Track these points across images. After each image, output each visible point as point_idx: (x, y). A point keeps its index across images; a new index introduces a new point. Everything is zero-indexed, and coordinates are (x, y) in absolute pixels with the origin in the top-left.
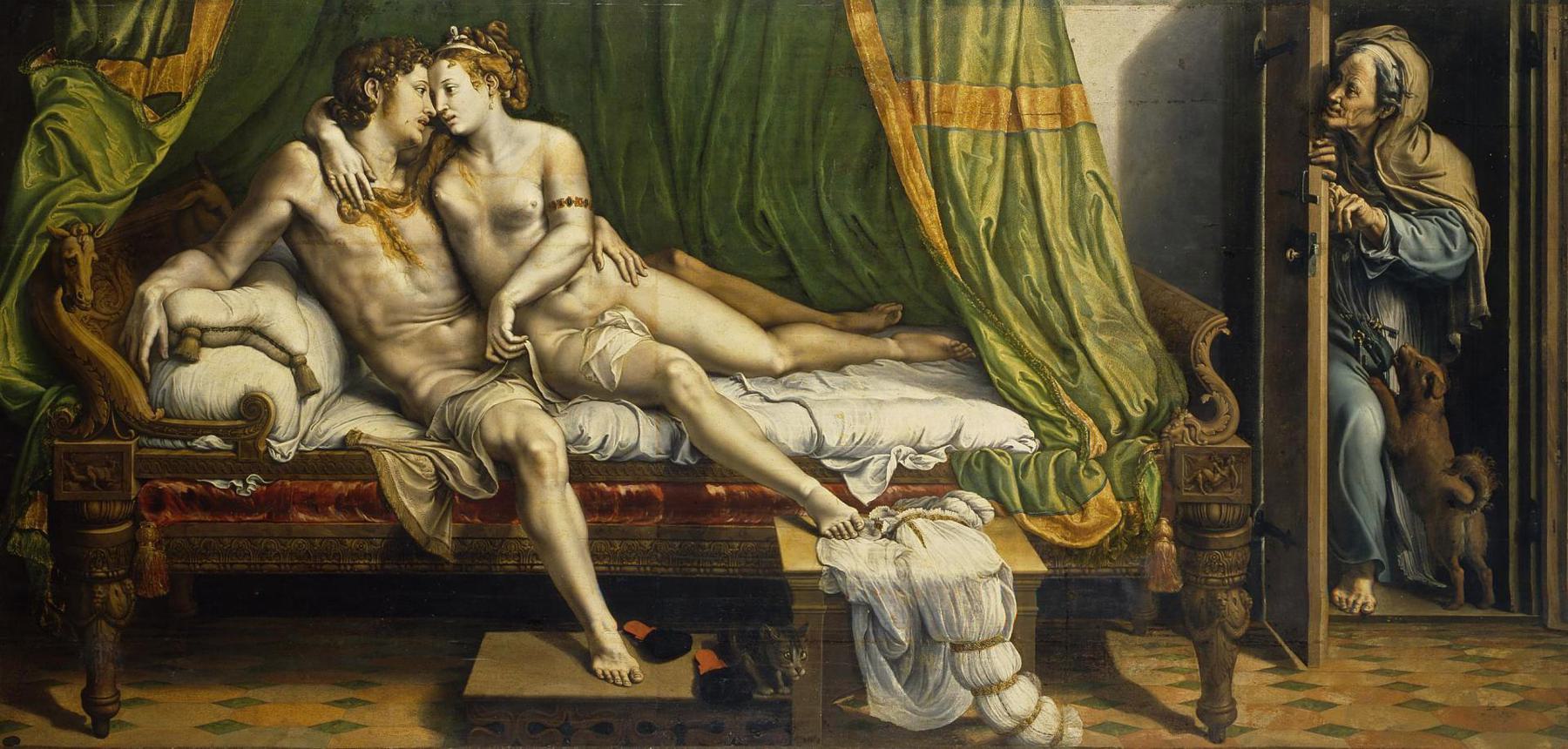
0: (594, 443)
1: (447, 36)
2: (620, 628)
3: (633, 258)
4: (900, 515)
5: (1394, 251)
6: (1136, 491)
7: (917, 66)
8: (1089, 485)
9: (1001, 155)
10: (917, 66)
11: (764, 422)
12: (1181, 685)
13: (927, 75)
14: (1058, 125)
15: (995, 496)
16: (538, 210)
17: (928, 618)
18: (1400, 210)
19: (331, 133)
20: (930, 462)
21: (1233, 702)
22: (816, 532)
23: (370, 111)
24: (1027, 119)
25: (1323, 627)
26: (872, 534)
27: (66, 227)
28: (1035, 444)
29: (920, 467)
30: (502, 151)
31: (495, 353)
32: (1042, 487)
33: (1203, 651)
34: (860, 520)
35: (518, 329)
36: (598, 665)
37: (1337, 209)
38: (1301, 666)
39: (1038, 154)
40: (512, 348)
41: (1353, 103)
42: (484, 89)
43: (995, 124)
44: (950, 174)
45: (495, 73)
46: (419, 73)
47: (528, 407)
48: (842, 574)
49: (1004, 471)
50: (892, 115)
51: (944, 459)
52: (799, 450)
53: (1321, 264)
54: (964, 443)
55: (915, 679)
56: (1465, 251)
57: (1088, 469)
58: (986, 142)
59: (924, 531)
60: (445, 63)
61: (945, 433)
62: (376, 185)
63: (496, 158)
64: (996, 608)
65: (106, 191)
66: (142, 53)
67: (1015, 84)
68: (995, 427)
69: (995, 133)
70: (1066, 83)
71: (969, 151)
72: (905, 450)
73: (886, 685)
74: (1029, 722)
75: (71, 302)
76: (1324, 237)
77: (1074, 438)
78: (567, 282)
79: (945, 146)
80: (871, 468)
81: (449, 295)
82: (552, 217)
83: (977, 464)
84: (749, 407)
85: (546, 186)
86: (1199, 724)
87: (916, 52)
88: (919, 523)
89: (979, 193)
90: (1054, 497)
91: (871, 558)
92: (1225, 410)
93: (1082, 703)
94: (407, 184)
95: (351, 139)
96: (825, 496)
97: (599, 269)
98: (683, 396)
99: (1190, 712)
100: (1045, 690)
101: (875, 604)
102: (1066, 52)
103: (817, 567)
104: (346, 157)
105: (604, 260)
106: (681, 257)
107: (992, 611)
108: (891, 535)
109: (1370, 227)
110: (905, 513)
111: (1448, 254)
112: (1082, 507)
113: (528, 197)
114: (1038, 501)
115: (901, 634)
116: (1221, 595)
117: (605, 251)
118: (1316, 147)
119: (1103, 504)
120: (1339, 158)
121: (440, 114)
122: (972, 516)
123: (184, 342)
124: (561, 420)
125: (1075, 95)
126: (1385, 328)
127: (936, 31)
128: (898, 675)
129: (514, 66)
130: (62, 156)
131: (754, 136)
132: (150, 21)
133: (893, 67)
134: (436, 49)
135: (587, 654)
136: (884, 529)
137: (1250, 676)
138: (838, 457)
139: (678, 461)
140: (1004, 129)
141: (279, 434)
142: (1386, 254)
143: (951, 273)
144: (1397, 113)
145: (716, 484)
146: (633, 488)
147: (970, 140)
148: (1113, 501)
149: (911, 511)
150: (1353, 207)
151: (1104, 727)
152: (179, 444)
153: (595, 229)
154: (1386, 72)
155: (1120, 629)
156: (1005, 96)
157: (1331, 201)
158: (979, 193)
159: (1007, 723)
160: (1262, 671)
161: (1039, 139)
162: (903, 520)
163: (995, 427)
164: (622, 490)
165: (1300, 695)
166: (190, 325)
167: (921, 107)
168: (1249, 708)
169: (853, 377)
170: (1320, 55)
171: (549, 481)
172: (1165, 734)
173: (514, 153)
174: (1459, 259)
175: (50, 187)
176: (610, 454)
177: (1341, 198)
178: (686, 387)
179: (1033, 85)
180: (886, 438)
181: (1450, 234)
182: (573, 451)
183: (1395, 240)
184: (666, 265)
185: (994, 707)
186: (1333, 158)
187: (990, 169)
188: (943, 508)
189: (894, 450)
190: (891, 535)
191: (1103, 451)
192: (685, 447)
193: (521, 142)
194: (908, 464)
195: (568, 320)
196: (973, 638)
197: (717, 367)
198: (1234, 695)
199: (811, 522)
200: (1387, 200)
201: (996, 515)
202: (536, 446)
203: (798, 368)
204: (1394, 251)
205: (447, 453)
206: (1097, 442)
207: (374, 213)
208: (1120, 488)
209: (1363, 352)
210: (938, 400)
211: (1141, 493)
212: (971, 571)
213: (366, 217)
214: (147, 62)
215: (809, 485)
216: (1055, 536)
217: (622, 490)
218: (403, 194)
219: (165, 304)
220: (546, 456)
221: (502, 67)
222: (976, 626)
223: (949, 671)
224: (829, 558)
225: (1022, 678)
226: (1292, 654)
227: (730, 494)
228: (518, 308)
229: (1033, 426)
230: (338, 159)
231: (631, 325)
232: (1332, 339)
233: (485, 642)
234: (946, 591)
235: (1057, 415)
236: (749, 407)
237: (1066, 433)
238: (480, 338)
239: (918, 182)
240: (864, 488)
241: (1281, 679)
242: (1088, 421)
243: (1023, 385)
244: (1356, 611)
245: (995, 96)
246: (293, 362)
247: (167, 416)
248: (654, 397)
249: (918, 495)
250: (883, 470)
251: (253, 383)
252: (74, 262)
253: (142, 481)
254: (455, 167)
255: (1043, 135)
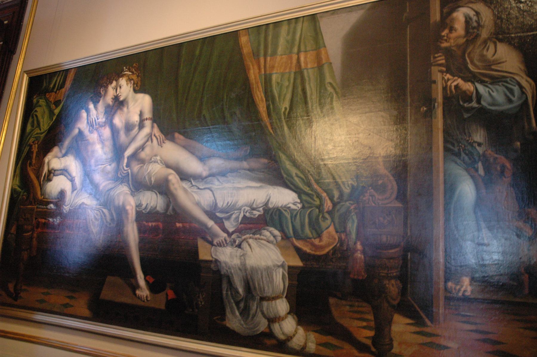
0: (144, 206)
1: (123, 70)
2: (145, 279)
3: (162, 136)
4: (243, 237)
5: (479, 102)
6: (345, 228)
7: (262, 52)
8: (324, 225)
9: (292, 81)
10: (262, 52)
11: (196, 197)
12: (364, 328)
13: (265, 56)
14: (316, 65)
15: (282, 230)
16: (138, 123)
17: (251, 283)
18: (482, 82)
19: (91, 106)
20: (257, 213)
21: (391, 340)
22: (211, 243)
23: (101, 97)
24: (303, 65)
25: (442, 303)
26: (232, 245)
27: (33, 142)
28: (300, 206)
29: (252, 216)
30: (131, 104)
31: (121, 174)
32: (303, 225)
33: (376, 310)
34: (228, 240)
35: (128, 165)
36: (138, 292)
37: (446, 86)
38: (429, 323)
39: (307, 78)
40: (125, 172)
41: (454, 35)
42: (129, 85)
43: (290, 68)
44: (271, 91)
45: (132, 79)
46: (114, 83)
47: (127, 193)
48: (220, 262)
49: (286, 218)
50: (252, 71)
51: (262, 212)
52: (208, 209)
53: (439, 112)
54: (271, 206)
55: (245, 312)
56: (520, 98)
57: (323, 217)
58: (286, 76)
59: (252, 245)
60: (121, 79)
61: (263, 200)
62: (99, 120)
63: (129, 107)
64: (279, 281)
65: (42, 131)
66: (55, 90)
67: (299, 52)
68: (283, 197)
69: (290, 73)
70: (319, 48)
71: (279, 81)
72: (247, 208)
73: (233, 313)
74: (291, 338)
75: (31, 164)
76: (440, 99)
77: (318, 202)
78: (142, 147)
79: (270, 79)
80: (234, 216)
81: (110, 155)
82: (141, 126)
83: (275, 215)
84: (193, 192)
85: (141, 114)
86: (373, 349)
87: (262, 47)
88: (250, 241)
89: (282, 98)
90: (307, 231)
91: (231, 256)
92: (390, 187)
93: (316, 331)
94: (107, 119)
95: (96, 108)
96: (217, 229)
97: (152, 142)
98: (172, 188)
99: (369, 342)
100: (300, 322)
101: (231, 275)
102: (320, 36)
103: (211, 259)
104: (93, 112)
105: (154, 138)
106: (177, 135)
107: (277, 283)
108: (239, 246)
109: (465, 92)
110: (245, 237)
111: (510, 101)
112: (319, 236)
113: (136, 119)
114: (300, 232)
115: (241, 290)
116: (386, 282)
117: (155, 135)
118: (435, 58)
119: (329, 233)
120: (446, 61)
121: (117, 95)
122: (272, 238)
123: (51, 173)
124: (135, 198)
125: (323, 52)
126: (475, 142)
127: (270, 38)
128: (238, 308)
129: (138, 76)
130: (35, 122)
131: (204, 87)
132: (58, 81)
133: (253, 54)
134: (119, 75)
135: (135, 287)
136: (237, 243)
137: (400, 326)
138: (222, 211)
139: (168, 213)
140: (293, 70)
141: (66, 204)
142: (474, 104)
143: (269, 132)
144: (478, 36)
145: (179, 223)
146: (154, 224)
147: (280, 77)
148: (334, 233)
149: (248, 236)
150: (455, 83)
151: (326, 345)
152: (45, 207)
153: (152, 127)
154: (471, 19)
155: (335, 296)
156: (295, 57)
157: (443, 81)
158: (282, 98)
159: (282, 337)
160: (408, 324)
161: (308, 73)
162: (245, 239)
163: (283, 197)
164: (150, 224)
165: (429, 340)
166: (52, 169)
167: (262, 67)
168: (400, 344)
169: (230, 178)
170: (436, 15)
171: (130, 221)
172: (355, 352)
173: (134, 105)
174: (517, 100)
175: (32, 130)
176: (148, 210)
177: (448, 80)
178: (173, 184)
179: (306, 51)
180: (240, 203)
181: (511, 91)
182: (137, 209)
183: (479, 97)
184: (172, 140)
185: (276, 328)
186: (443, 61)
187: (288, 87)
188: (260, 235)
189: (243, 208)
190: (239, 246)
191: (331, 208)
192: (171, 208)
193: (136, 101)
194: (248, 215)
195: (142, 162)
196: (269, 295)
197: (184, 176)
198: (393, 335)
199: (210, 239)
200: (472, 78)
201: (282, 239)
202: (128, 207)
203: (212, 175)
204: (479, 102)
205: (104, 210)
206: (328, 205)
207: (96, 130)
208: (338, 226)
209: (463, 155)
210: (261, 187)
211: (348, 229)
212: (270, 263)
213: (95, 131)
214: (56, 92)
215: (211, 223)
216: (307, 249)
217: (150, 224)
218: (105, 122)
219: (48, 163)
220: (130, 211)
221: (135, 77)
222: (271, 291)
223: (258, 310)
224: (216, 255)
225: (289, 316)
226: (424, 317)
227: (184, 227)
228: (128, 158)
229: (300, 197)
230: (91, 113)
231: (159, 162)
232: (446, 149)
233: (107, 279)
234: (259, 272)
235: (310, 192)
236: (193, 192)
237: (314, 201)
238: (118, 169)
239: (259, 96)
240: (230, 226)
241: (418, 329)
242: (324, 195)
243: (296, 179)
244: (460, 294)
245: (291, 58)
246: (72, 180)
247: (44, 198)
248: (162, 188)
249: (250, 229)
250: (237, 218)
251: (63, 188)
252: (32, 153)
253: (36, 219)
254: (119, 112)
255: (310, 71)
